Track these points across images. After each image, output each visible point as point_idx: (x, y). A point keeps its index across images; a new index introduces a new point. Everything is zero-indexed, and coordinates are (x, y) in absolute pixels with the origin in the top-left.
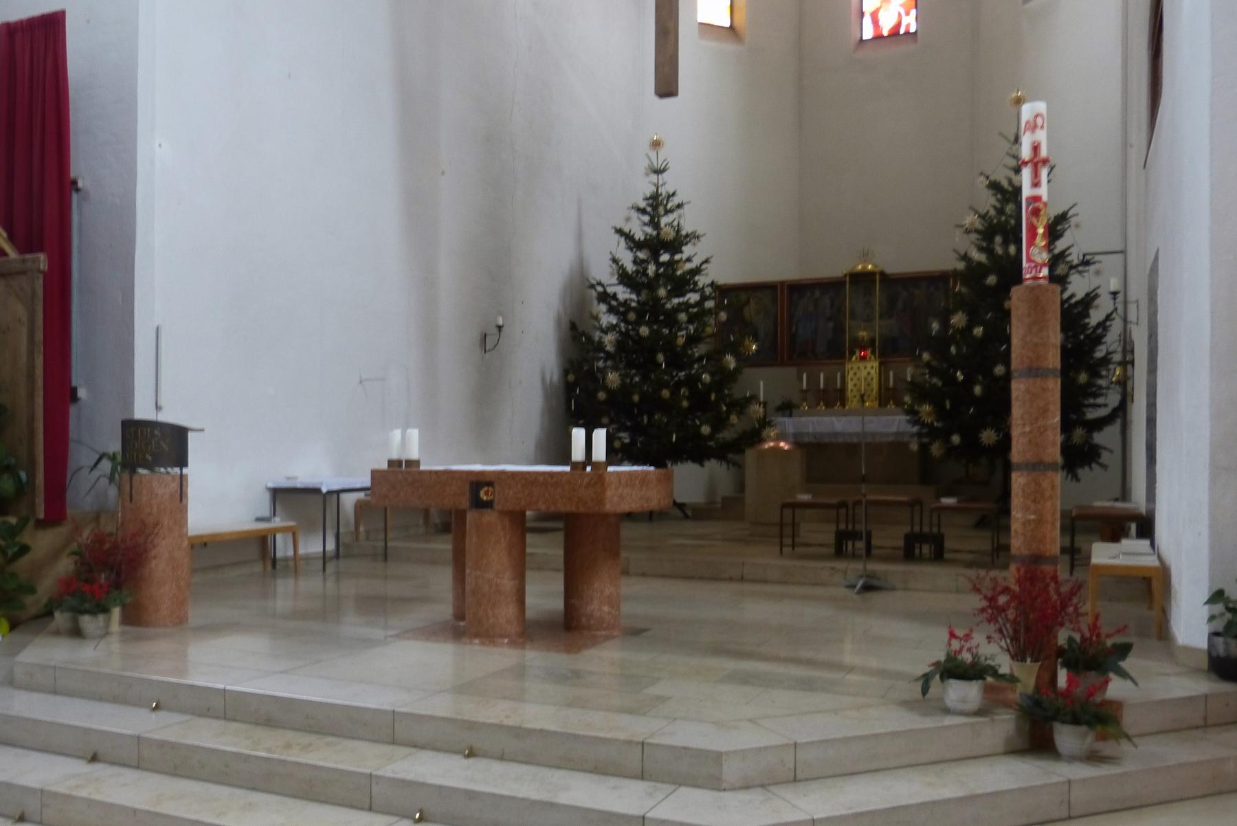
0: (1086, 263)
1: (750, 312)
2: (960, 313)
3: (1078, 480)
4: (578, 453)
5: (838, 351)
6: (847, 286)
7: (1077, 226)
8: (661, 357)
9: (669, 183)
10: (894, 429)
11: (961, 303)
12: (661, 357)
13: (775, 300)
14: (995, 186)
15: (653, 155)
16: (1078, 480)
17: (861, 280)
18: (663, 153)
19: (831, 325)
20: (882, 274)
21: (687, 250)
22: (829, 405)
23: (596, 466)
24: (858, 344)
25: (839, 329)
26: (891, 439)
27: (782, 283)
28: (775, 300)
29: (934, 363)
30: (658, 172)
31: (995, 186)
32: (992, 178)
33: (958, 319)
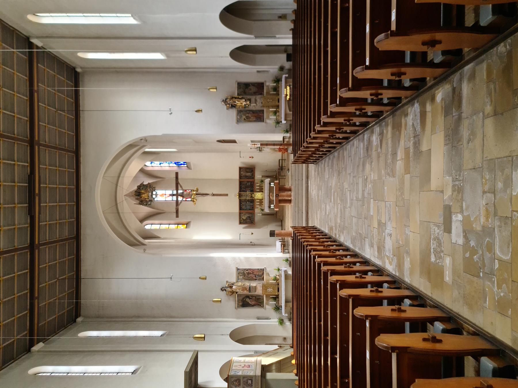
1: (244, 218)
5: (252, 201)
13: (242, 213)
17: (240, 196)
19: (247, 202)
24: (252, 197)
25: (248, 201)
28: (242, 213)
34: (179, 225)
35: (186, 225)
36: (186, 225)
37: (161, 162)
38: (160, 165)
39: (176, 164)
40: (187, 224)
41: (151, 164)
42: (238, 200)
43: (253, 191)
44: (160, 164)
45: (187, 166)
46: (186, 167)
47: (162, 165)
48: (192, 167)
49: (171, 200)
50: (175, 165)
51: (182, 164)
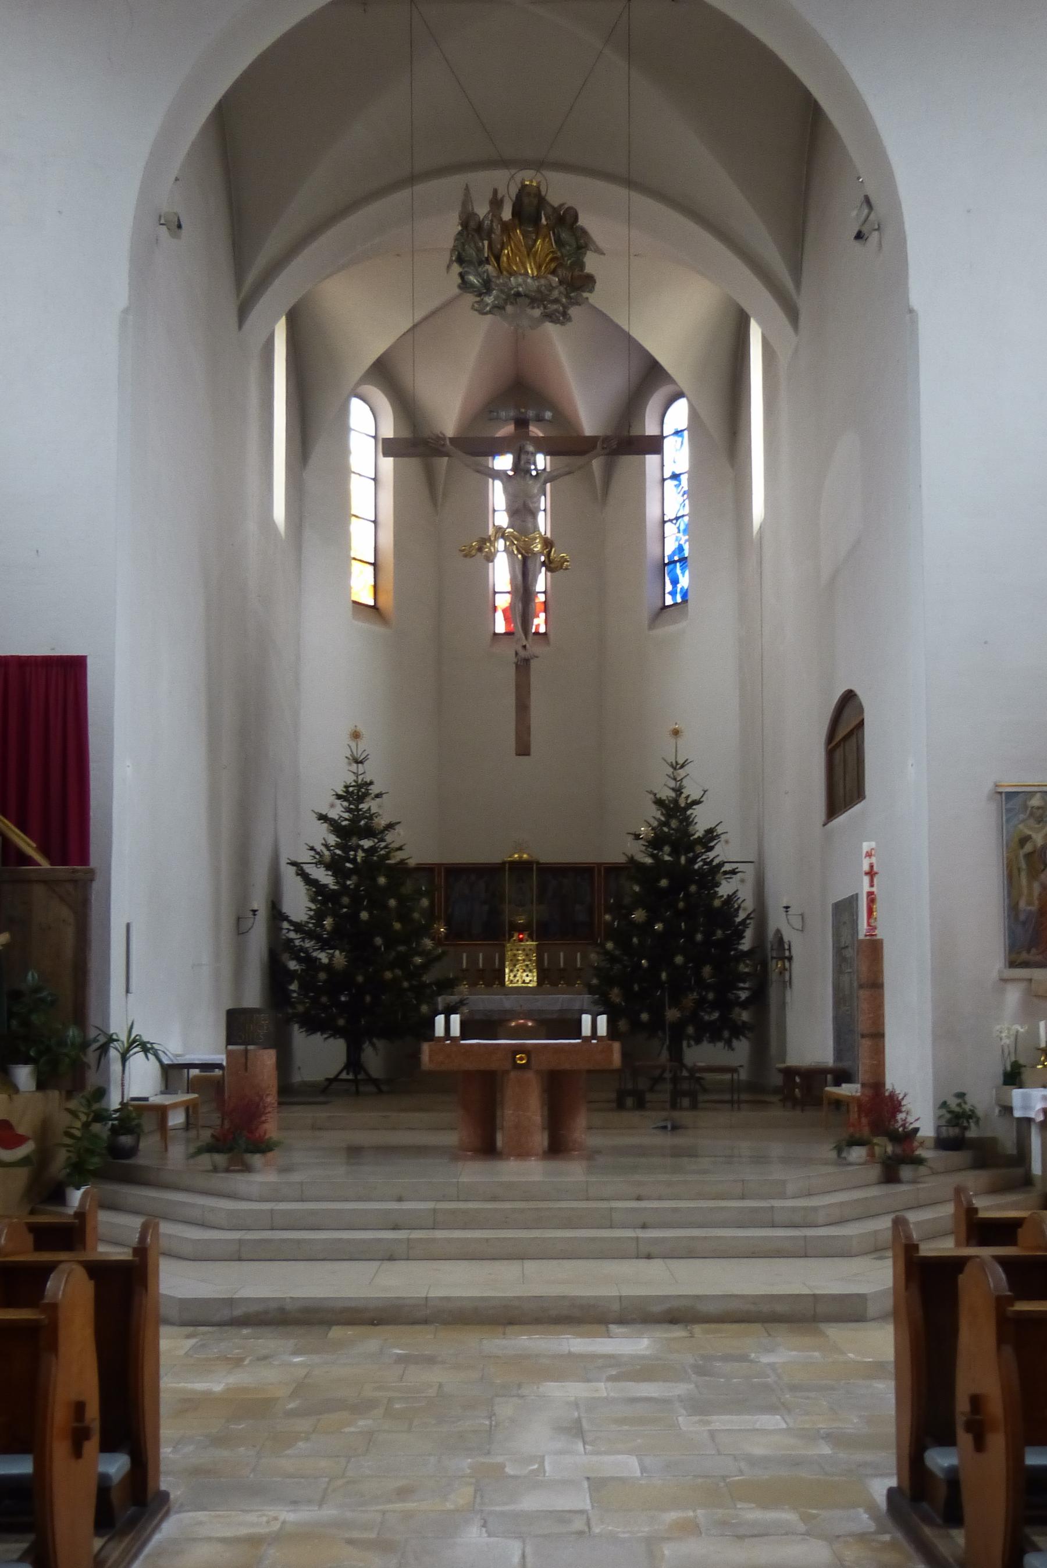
0: (734, 872)
2: (640, 910)
3: (733, 1050)
4: (586, 1031)
6: (507, 873)
7: (727, 842)
8: (378, 941)
9: (370, 772)
10: (558, 1007)
11: (639, 902)
12: (378, 941)
14: (659, 803)
15: (353, 745)
16: (733, 1050)
17: (521, 869)
18: (363, 744)
20: (538, 863)
21: (389, 837)
22: (489, 985)
23: (454, 1039)
24: (515, 928)
26: (555, 1016)
27: (440, 865)
29: (617, 953)
30: (358, 762)
31: (659, 803)
32: (658, 796)
33: (638, 915)
34: (370, 569)
35: (372, 603)
36: (372, 603)
37: (684, 479)
38: (667, 475)
39: (674, 554)
40: (375, 608)
41: (677, 433)
42: (496, 859)
43: (542, 932)
44: (675, 477)
45: (665, 607)
46: (660, 605)
47: (669, 485)
48: (660, 632)
49: (496, 509)
50: (670, 547)
51: (675, 582)
